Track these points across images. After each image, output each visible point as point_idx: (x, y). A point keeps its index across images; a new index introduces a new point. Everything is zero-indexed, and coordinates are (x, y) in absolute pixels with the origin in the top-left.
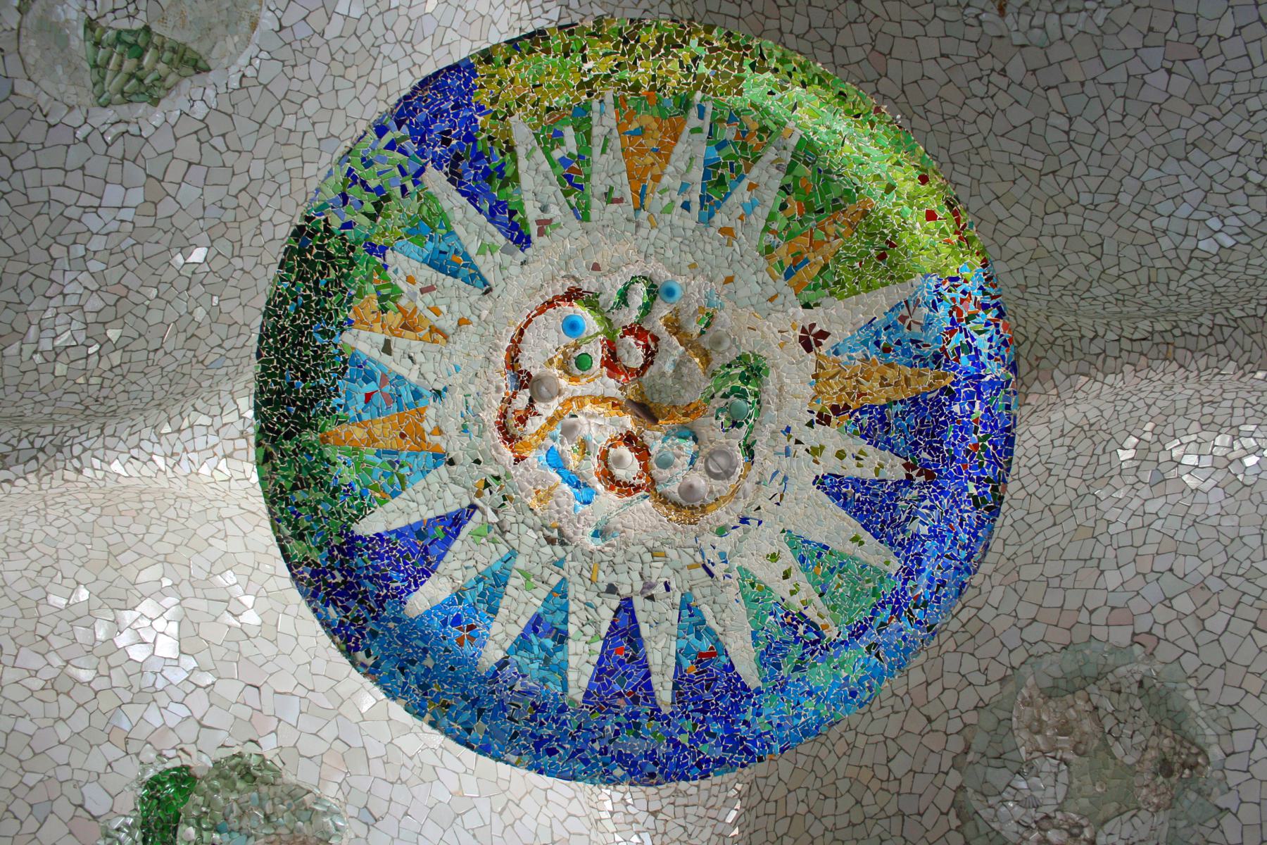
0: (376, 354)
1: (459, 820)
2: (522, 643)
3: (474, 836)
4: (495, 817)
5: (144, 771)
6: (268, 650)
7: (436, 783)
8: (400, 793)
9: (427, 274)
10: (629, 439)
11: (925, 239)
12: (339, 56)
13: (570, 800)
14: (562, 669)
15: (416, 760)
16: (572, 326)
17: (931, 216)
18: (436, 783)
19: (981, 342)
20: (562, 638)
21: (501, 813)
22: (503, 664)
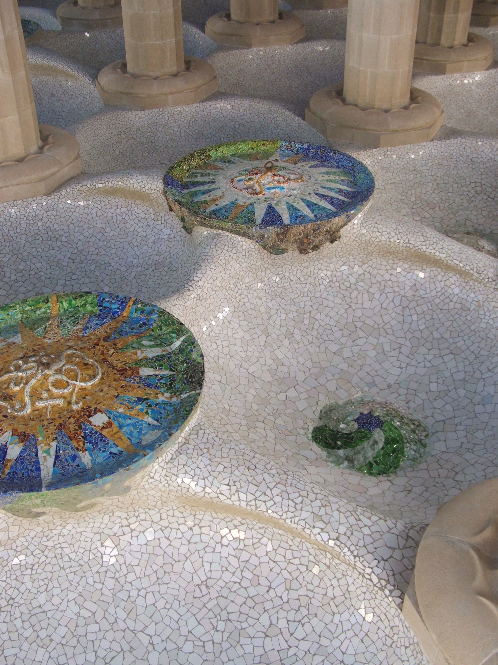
0: (216, 207)
1: (386, 353)
2: (313, 211)
3: (394, 349)
4: (388, 336)
5: (308, 437)
6: (285, 369)
7: (367, 353)
8: (367, 369)
9: (206, 196)
10: (274, 175)
11: (269, 147)
12: (116, 289)
13: (387, 297)
14: (324, 208)
15: (355, 355)
16: (240, 181)
17: (264, 144)
18: (367, 353)
19: (298, 146)
20: (316, 204)
21: (387, 334)
22: (315, 216)
